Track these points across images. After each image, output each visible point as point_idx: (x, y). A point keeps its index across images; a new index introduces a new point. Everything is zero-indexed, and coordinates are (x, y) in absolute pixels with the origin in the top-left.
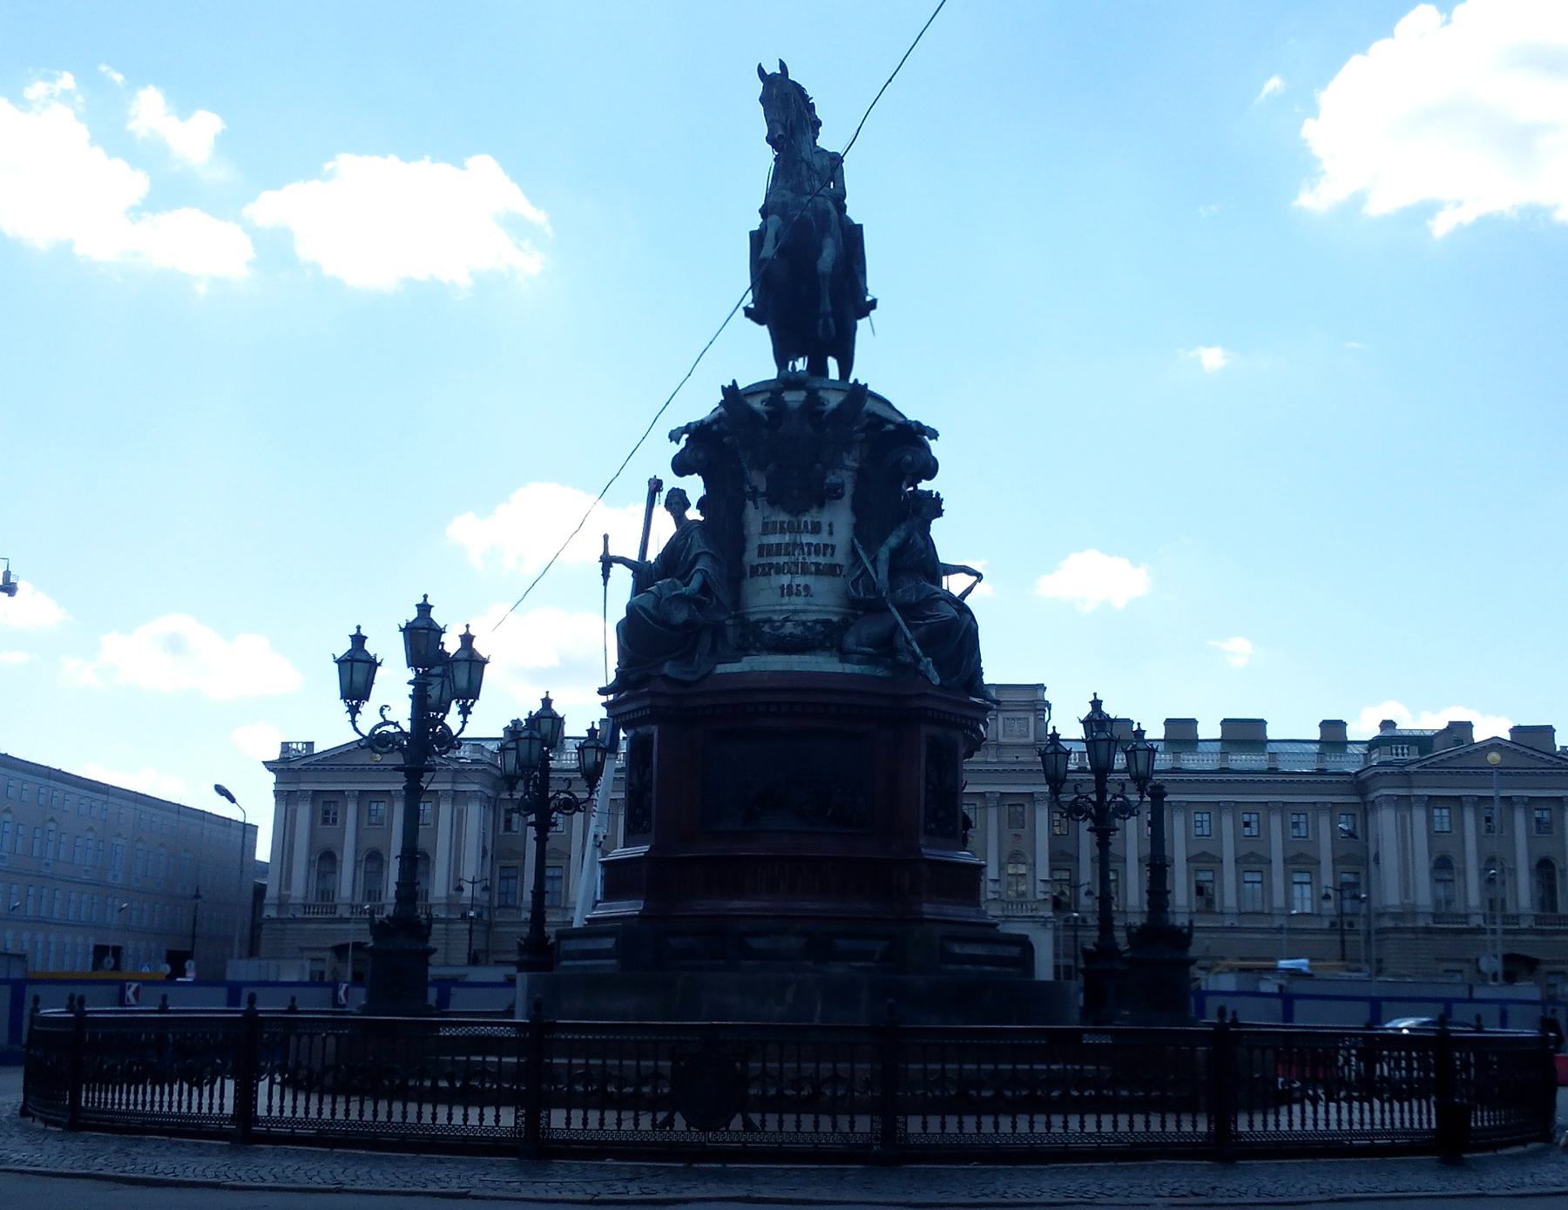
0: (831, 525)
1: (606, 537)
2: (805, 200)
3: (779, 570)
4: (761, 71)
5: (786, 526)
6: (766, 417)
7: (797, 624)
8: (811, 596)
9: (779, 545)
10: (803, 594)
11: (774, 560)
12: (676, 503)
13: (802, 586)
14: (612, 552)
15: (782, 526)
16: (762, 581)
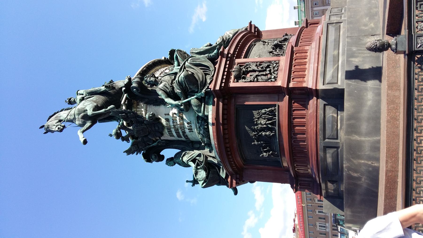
0: (165, 115)
1: (187, 181)
2: (77, 117)
3: (184, 133)
4: (45, 133)
5: (169, 130)
6: (134, 140)
7: (200, 130)
8: (191, 121)
9: (176, 133)
10: (190, 125)
11: (181, 134)
12: (170, 164)
13: (188, 125)
14: (192, 179)
15: (170, 131)
16: (190, 137)
